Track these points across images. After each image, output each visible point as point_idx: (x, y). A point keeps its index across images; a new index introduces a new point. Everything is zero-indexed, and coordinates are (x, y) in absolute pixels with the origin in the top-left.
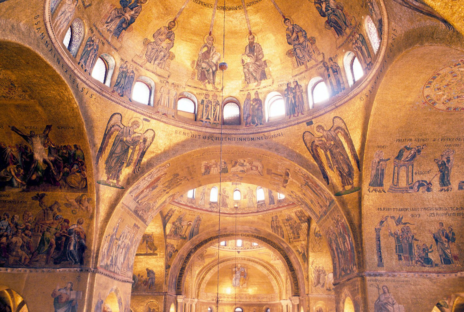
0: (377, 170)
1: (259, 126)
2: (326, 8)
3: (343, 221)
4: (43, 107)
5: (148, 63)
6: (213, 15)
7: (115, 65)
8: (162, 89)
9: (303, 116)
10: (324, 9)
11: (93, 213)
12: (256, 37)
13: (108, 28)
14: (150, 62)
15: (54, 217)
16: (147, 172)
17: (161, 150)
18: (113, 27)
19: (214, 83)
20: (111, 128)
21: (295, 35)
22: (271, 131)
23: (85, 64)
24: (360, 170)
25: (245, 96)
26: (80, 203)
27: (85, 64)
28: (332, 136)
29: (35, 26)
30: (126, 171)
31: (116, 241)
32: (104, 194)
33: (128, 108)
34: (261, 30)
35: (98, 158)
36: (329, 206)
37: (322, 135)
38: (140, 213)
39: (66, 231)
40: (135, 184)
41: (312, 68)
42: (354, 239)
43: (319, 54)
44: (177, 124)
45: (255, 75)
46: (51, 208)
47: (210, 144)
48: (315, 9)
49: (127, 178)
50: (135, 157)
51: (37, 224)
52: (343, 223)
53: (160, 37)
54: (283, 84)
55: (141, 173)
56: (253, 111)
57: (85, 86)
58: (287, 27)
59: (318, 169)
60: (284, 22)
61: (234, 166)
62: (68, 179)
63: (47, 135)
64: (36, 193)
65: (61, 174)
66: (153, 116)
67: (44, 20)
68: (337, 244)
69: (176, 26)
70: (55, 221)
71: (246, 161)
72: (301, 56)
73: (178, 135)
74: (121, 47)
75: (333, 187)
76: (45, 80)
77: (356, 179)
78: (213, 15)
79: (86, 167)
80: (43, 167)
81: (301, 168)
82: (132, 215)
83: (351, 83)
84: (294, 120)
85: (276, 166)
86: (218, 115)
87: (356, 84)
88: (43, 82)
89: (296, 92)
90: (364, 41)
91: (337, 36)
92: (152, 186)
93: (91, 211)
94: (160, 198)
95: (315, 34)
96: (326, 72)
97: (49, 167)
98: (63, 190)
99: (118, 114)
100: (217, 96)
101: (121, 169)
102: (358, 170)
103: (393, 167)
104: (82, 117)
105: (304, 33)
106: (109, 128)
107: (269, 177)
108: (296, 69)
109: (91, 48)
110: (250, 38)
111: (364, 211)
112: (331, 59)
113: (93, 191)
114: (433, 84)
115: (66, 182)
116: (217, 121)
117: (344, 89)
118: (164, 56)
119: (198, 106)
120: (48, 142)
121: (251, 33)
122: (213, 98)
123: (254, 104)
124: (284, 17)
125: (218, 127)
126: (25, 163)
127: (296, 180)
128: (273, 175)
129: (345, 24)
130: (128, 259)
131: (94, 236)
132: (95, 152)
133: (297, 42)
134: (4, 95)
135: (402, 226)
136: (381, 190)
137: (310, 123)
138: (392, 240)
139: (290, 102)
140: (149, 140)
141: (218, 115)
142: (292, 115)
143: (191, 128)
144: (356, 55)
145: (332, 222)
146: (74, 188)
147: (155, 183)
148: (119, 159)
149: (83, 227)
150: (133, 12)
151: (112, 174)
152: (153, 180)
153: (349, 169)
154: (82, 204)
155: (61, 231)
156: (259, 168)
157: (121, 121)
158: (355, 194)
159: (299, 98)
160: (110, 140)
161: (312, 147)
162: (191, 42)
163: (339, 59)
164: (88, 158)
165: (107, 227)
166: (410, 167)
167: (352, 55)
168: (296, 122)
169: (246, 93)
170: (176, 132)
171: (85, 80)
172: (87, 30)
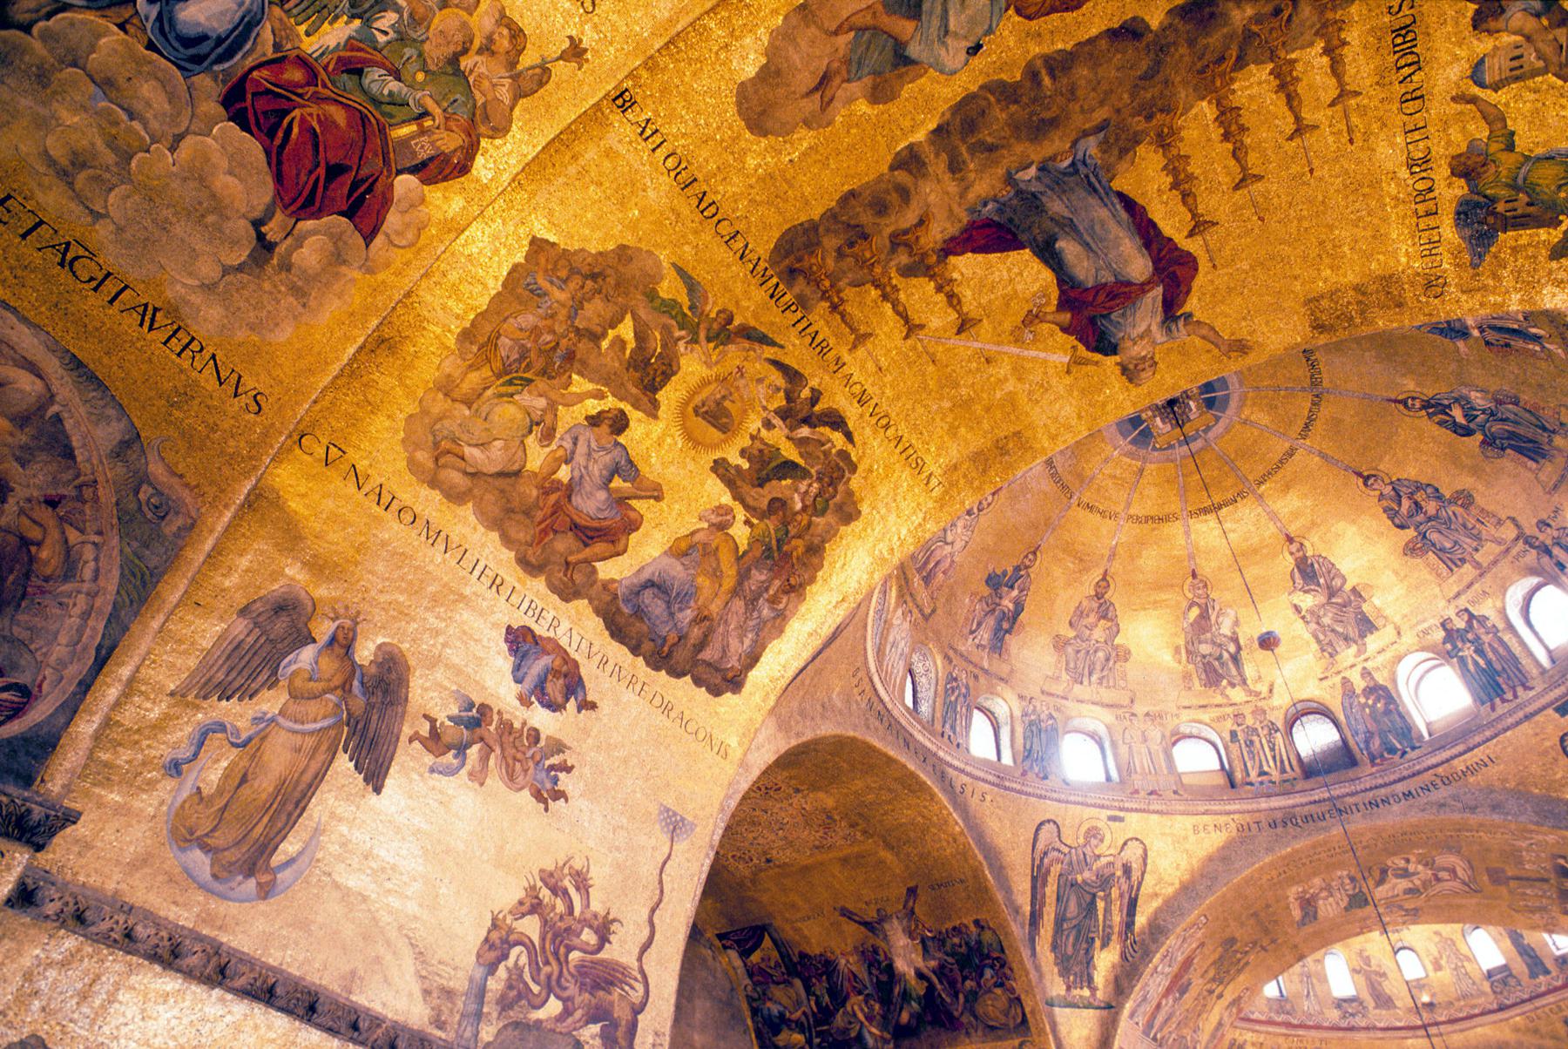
2: (1465, 416)
4: (893, 848)
5: (1077, 687)
6: (1187, 533)
9: (1532, 693)
10: (1460, 419)
12: (1307, 543)
14: (1081, 683)
17: (1172, 884)
18: (986, 636)
19: (1244, 682)
20: (1042, 860)
21: (1406, 504)
25: (1339, 692)
29: (855, 690)
30: (1105, 961)
32: (1069, 1032)
33: (1067, 802)
34: (1313, 523)
35: (1032, 941)
40: (1137, 989)
41: (1495, 562)
43: (1500, 523)
44: (1191, 808)
45: (1340, 630)
49: (1112, 978)
50: (1117, 918)
53: (1086, 621)
54: (1430, 628)
56: (1376, 721)
57: (965, 779)
58: (1378, 493)
60: (1365, 484)
61: (1381, 882)
63: (912, 912)
66: (1127, 805)
69: (1112, 586)
71: (1413, 859)
72: (1448, 545)
73: (1202, 834)
74: (1012, 671)
76: (890, 790)
79: (1011, 969)
80: (919, 988)
84: (1511, 713)
86: (1285, 758)
88: (885, 796)
89: (1478, 638)
92: (1178, 985)
94: (1205, 1016)
95: (1466, 482)
97: (931, 988)
99: (1049, 821)
101: (1092, 957)
104: (977, 851)
105: (1429, 490)
109: (956, 693)
110: (1294, 550)
113: (1043, 1030)
115: (976, 1017)
116: (1290, 774)
118: (1108, 660)
119: (1226, 748)
120: (917, 926)
122: (1255, 719)
123: (1370, 702)
124: (1359, 475)
125: (1298, 788)
126: (879, 985)
128: (1513, 884)
132: (1023, 928)
133: (1420, 518)
134: (817, 843)
139: (1471, 667)
141: (1285, 758)
142: (1497, 700)
143: (1228, 808)
146: (997, 1028)
147: (1182, 977)
150: (1015, 593)
151: (1075, 974)
152: (1175, 968)
156: (1460, 873)
157: (1059, 836)
159: (1495, 651)
162: (1155, 609)
164: (1011, 946)
168: (1521, 714)
169: (1337, 679)
170: (1195, 829)
171: (962, 766)
172: (939, 662)
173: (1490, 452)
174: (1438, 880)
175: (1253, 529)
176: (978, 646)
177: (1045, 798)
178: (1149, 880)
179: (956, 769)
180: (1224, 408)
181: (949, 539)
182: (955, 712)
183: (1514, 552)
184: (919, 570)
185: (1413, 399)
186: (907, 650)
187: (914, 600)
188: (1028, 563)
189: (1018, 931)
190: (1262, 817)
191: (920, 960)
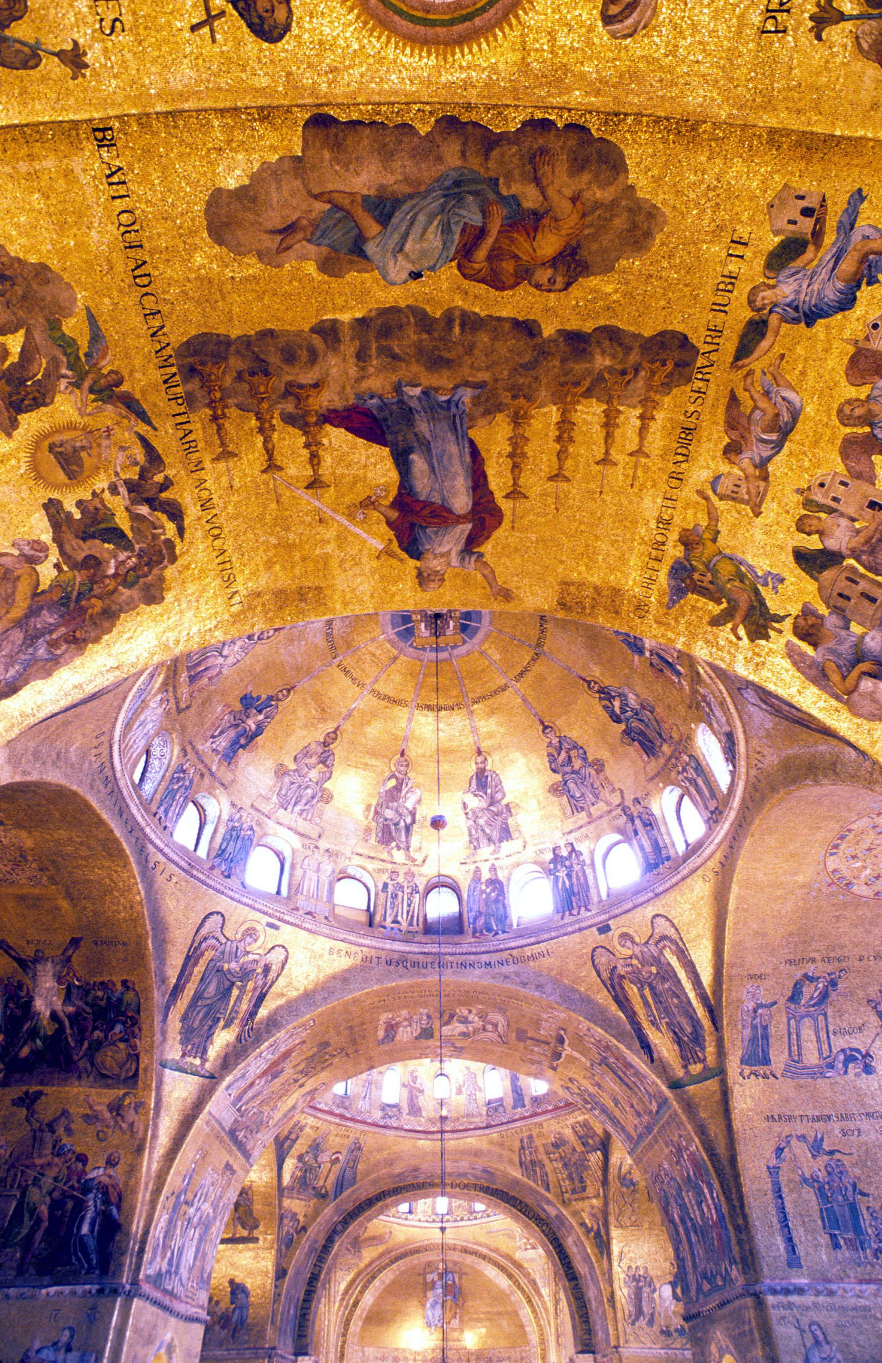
0: (754, 1027)
1: (501, 936)
3: (693, 1148)
5: (282, 811)
6: (410, 720)
7: (220, 817)
8: (306, 862)
9: (589, 914)
11: (144, 1139)
12: (490, 760)
13: (214, 746)
15: (54, 1147)
16: (267, 1040)
18: (223, 744)
20: (201, 943)
21: (563, 755)
22: (526, 946)
23: (166, 816)
24: (717, 1029)
26: (118, 1114)
27: (166, 816)
28: (653, 957)
29: (94, 751)
31: (184, 1207)
33: (239, 902)
35: (167, 1009)
36: (657, 1112)
37: (630, 952)
38: (241, 1135)
39: (76, 1185)
40: (240, 1067)
41: (601, 817)
42: (724, 1193)
43: (613, 790)
44: (334, 934)
45: (488, 831)
46: (51, 1127)
47: (401, 976)
48: (601, 708)
49: (223, 1054)
50: (244, 1006)
51: (13, 1166)
52: (692, 1154)
53: (307, 761)
55: (253, 1043)
56: (487, 905)
59: (629, 1027)
60: (543, 731)
61: (447, 1023)
62: (98, 1059)
63: (69, 960)
64: (24, 1089)
65: (86, 1045)
66: (286, 918)
67: (111, 738)
68: (683, 1207)
69: (339, 739)
70: (56, 1160)
71: (474, 1011)
72: (578, 795)
73: (335, 956)
74: (233, 781)
75: (664, 1068)
76: (89, 848)
77: (710, 1049)
78: (410, 720)
79: (140, 1030)
81: (592, 1025)
82: (224, 1142)
83: (681, 848)
84: (571, 924)
85: (537, 1023)
87: (693, 850)
88: (84, 852)
89: (571, 866)
90: (700, 768)
91: (645, 757)
92: (273, 1071)
93: (141, 1133)
94: (284, 1099)
95: (604, 754)
96: (629, 825)
97: (61, 1029)
98: (83, 1083)
99: (218, 913)
100: (413, 875)
102: (713, 1029)
103: (785, 1019)
105: (581, 751)
106: (196, 944)
107: (521, 1045)
108: (571, 820)
111: (737, 1124)
112: (637, 801)
113: (150, 1086)
114: (842, 847)
115: (92, 1064)
116: (415, 928)
117: (668, 858)
118: (313, 797)
119: (376, 895)
120: (68, 974)
121: (479, 752)
124: (542, 723)
125: (416, 940)
127: (580, 1053)
129: (661, 736)
130: (205, 1255)
131: (140, 1195)
133: (568, 769)
135: (826, 1158)
136: (768, 1072)
137: (604, 929)
138: (810, 1195)
139: (560, 885)
140: (275, 968)
142: (567, 913)
143: (362, 941)
144: (686, 792)
145: (667, 1151)
146: (109, 1077)
147: (278, 1064)
148: (210, 1010)
149: (118, 1173)
150: (261, 717)
151: (193, 1045)
153: (694, 1026)
154: (123, 1117)
155: (65, 1184)
156: (500, 1028)
157: (222, 928)
158: (713, 1085)
159: (578, 878)
160: (196, 969)
161: (611, 979)
162: (365, 770)
163: (653, 801)
165: (172, 1171)
166: (821, 1018)
167: (677, 792)
168: (577, 926)
169: (472, 867)
170: (331, 952)
171: (162, 846)
173: (627, 740)
174: (484, 1029)
175: (457, 734)
176: (213, 750)
177: (222, 893)
178: (281, 981)
179: (156, 847)
180: (471, 638)
181: (225, 652)
182: (173, 799)
183: (614, 813)
184: (189, 669)
185: (596, 683)
186: (152, 732)
187: (175, 691)
188: (280, 697)
189: (158, 997)
190: (383, 954)
191: (60, 1003)
